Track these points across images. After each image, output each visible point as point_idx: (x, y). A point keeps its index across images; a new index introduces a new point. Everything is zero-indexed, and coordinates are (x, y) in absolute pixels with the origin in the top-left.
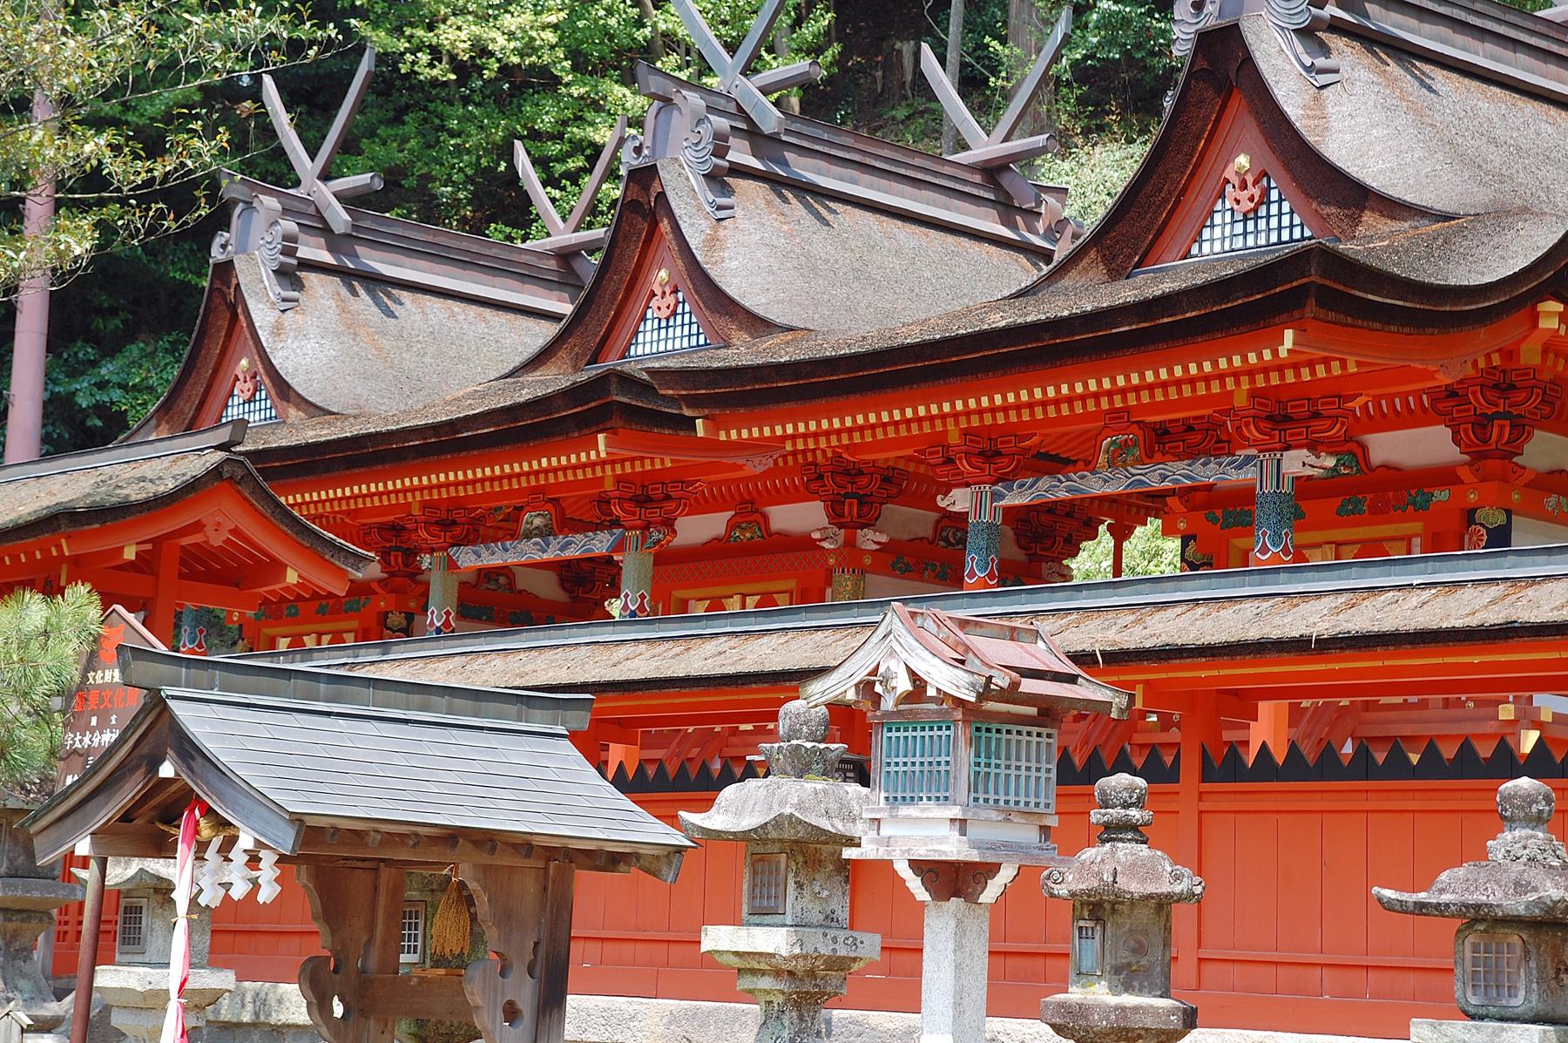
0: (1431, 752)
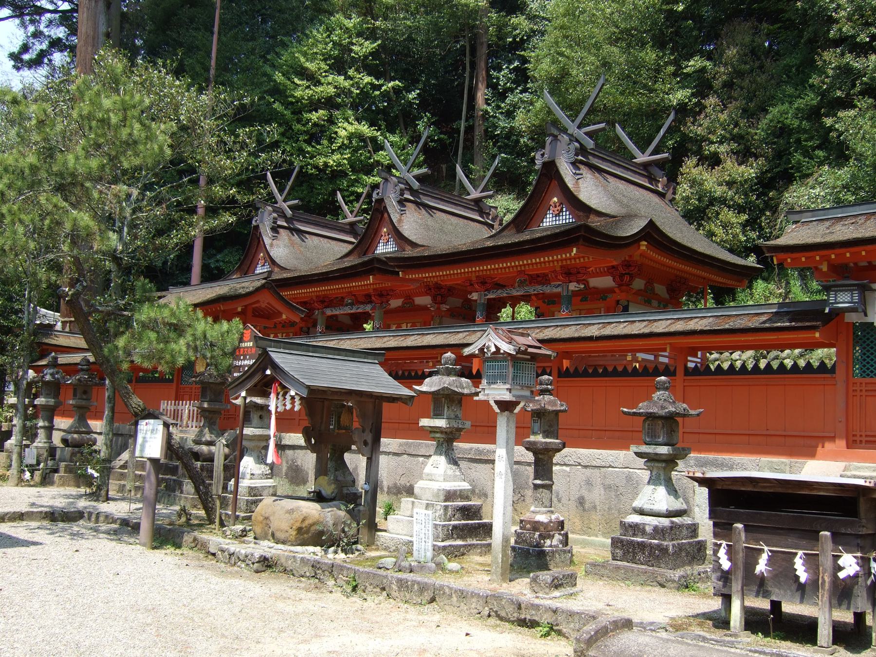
0: (605, 369)
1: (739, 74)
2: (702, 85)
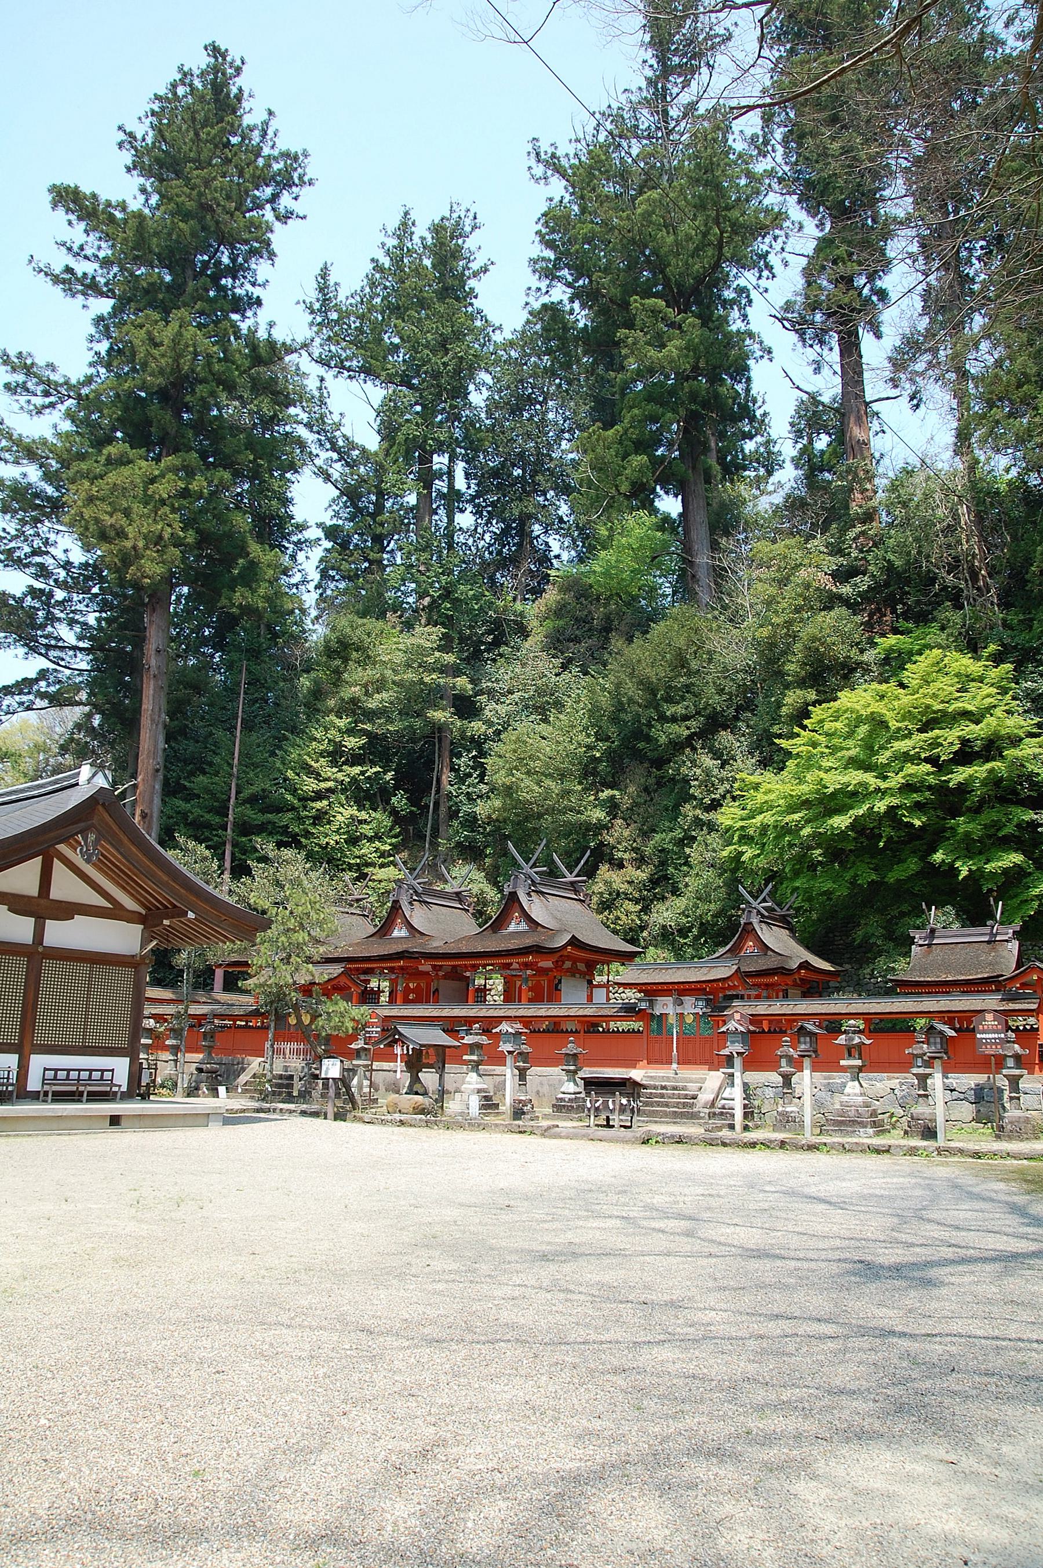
1: (636, 804)
2: (612, 807)
